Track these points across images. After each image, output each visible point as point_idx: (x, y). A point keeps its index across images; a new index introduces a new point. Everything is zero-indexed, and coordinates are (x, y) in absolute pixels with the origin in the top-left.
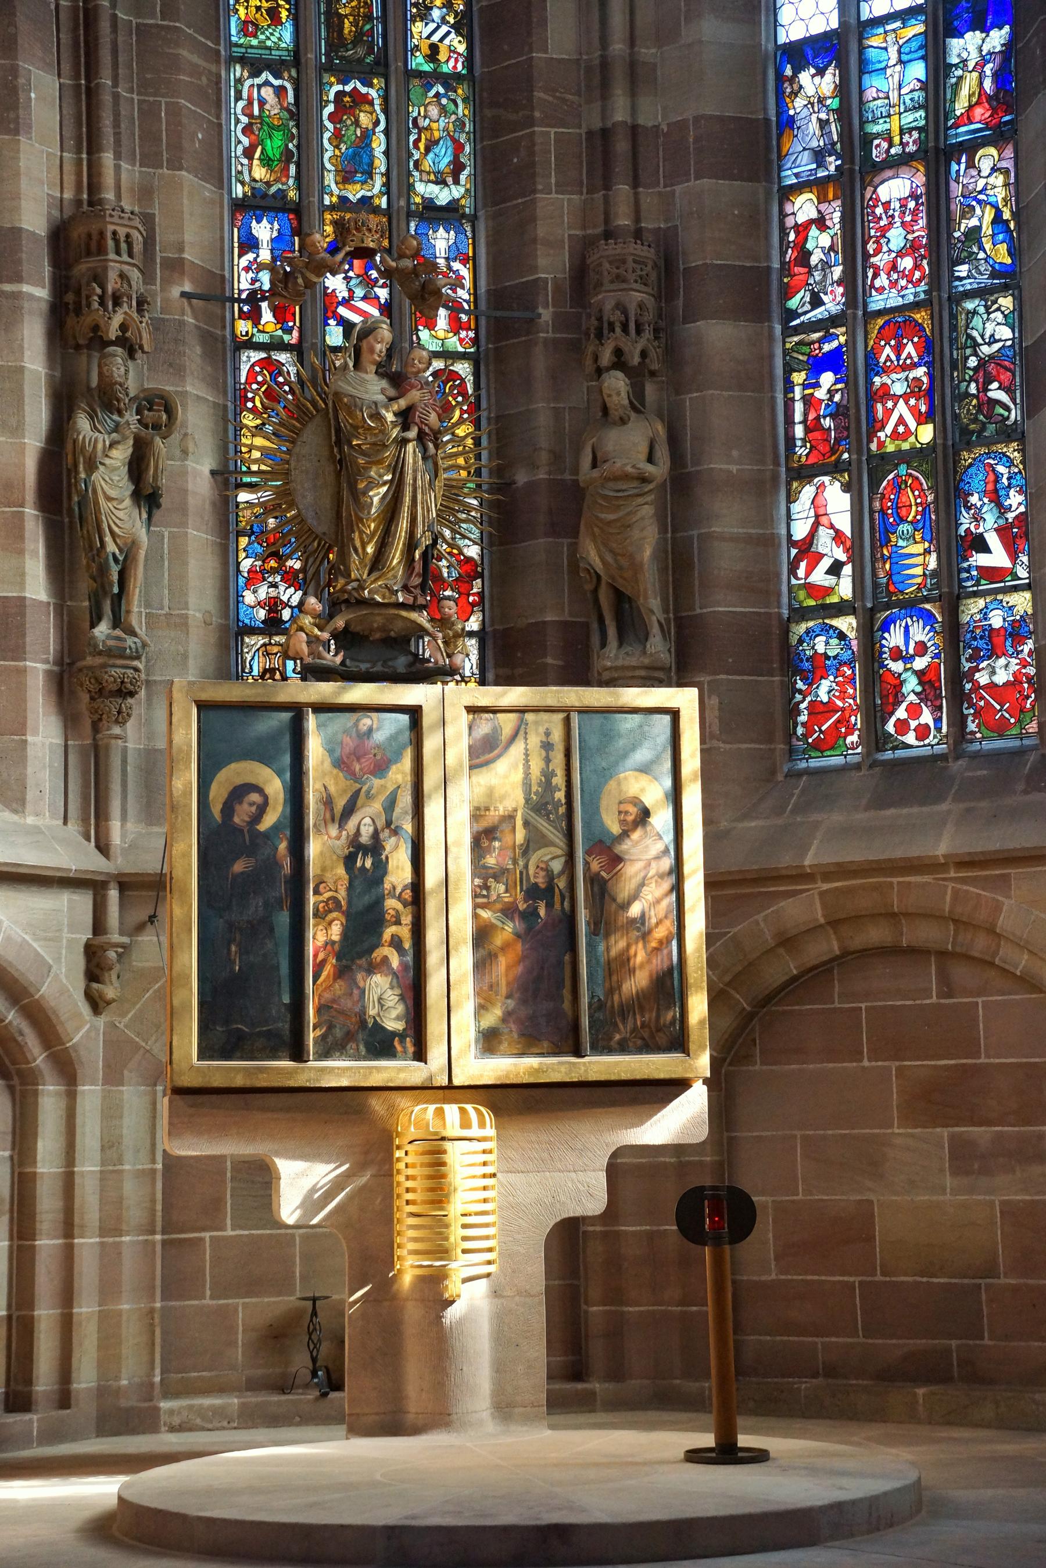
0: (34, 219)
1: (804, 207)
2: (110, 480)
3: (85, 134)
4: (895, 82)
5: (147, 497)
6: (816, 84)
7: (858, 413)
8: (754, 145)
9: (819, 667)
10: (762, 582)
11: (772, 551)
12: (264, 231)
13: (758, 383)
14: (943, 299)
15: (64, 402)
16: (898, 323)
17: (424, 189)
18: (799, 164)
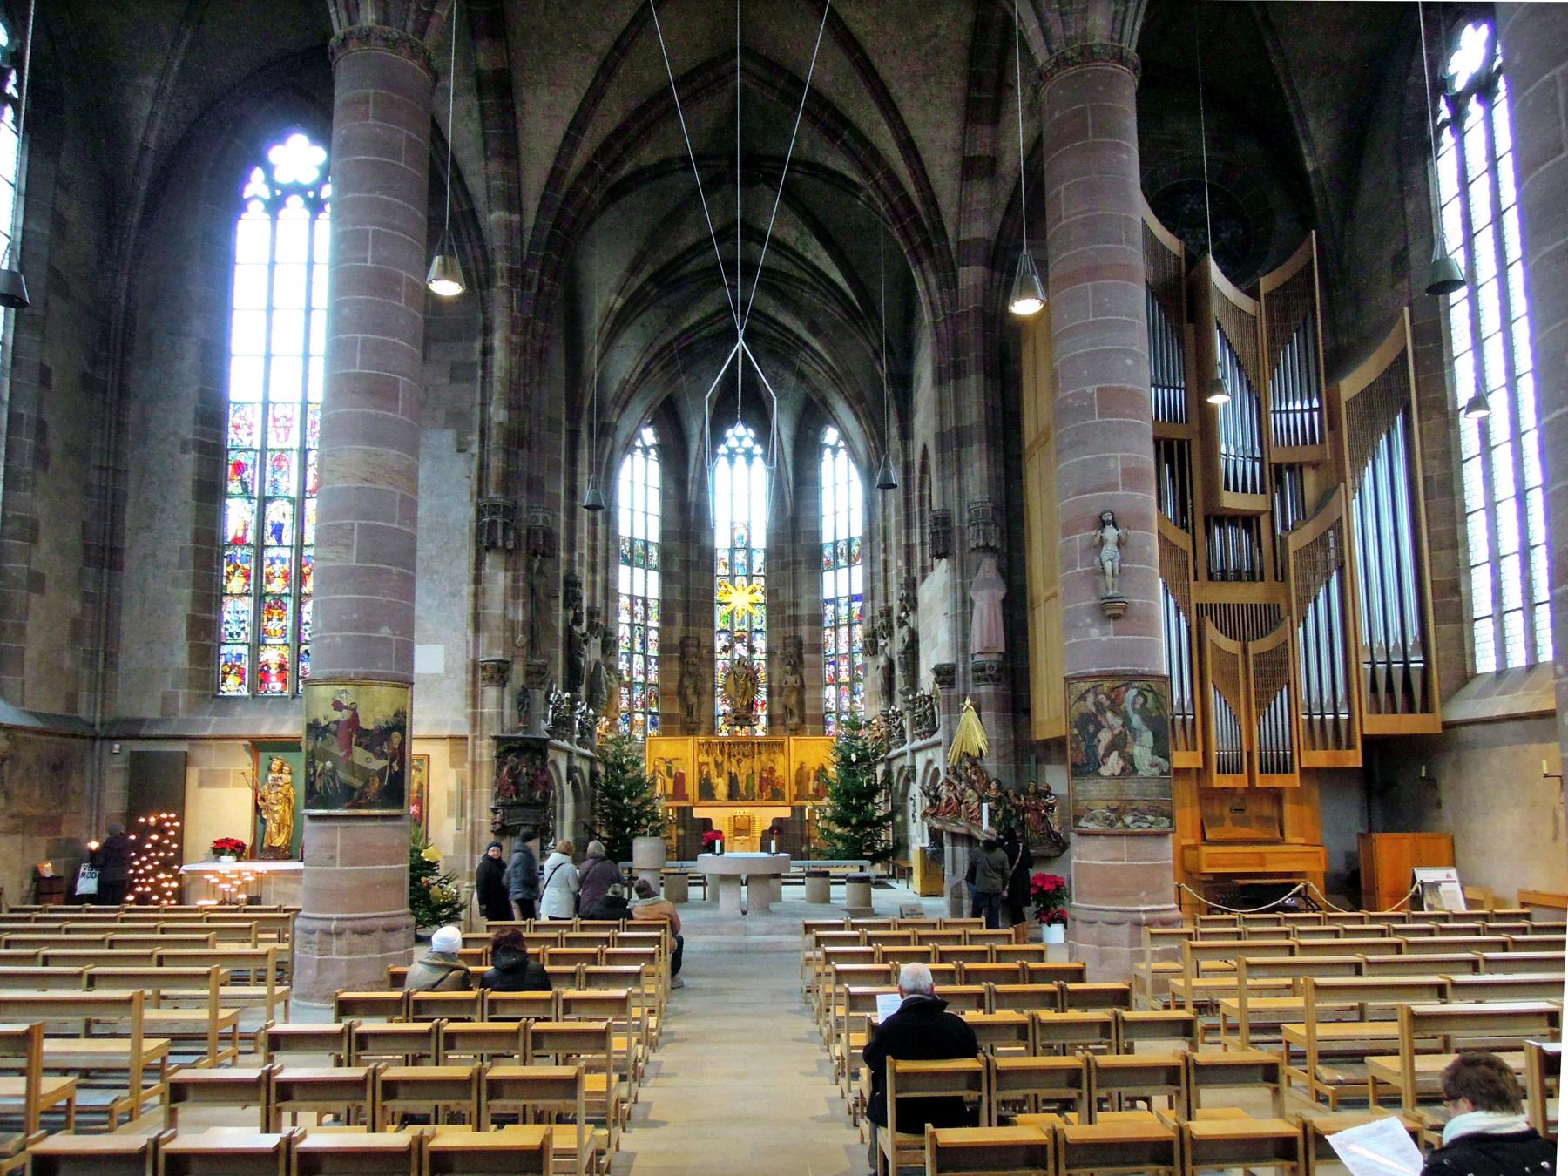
0: (676, 641)
1: (828, 632)
2: (690, 691)
3: (687, 624)
4: (843, 611)
5: (698, 693)
6: (829, 608)
7: (837, 674)
8: (817, 620)
9: (829, 724)
10: (819, 707)
11: (820, 700)
12: (723, 636)
13: (818, 667)
14: (851, 654)
15: (682, 675)
16: (844, 657)
17: (755, 626)
18: (827, 624)
